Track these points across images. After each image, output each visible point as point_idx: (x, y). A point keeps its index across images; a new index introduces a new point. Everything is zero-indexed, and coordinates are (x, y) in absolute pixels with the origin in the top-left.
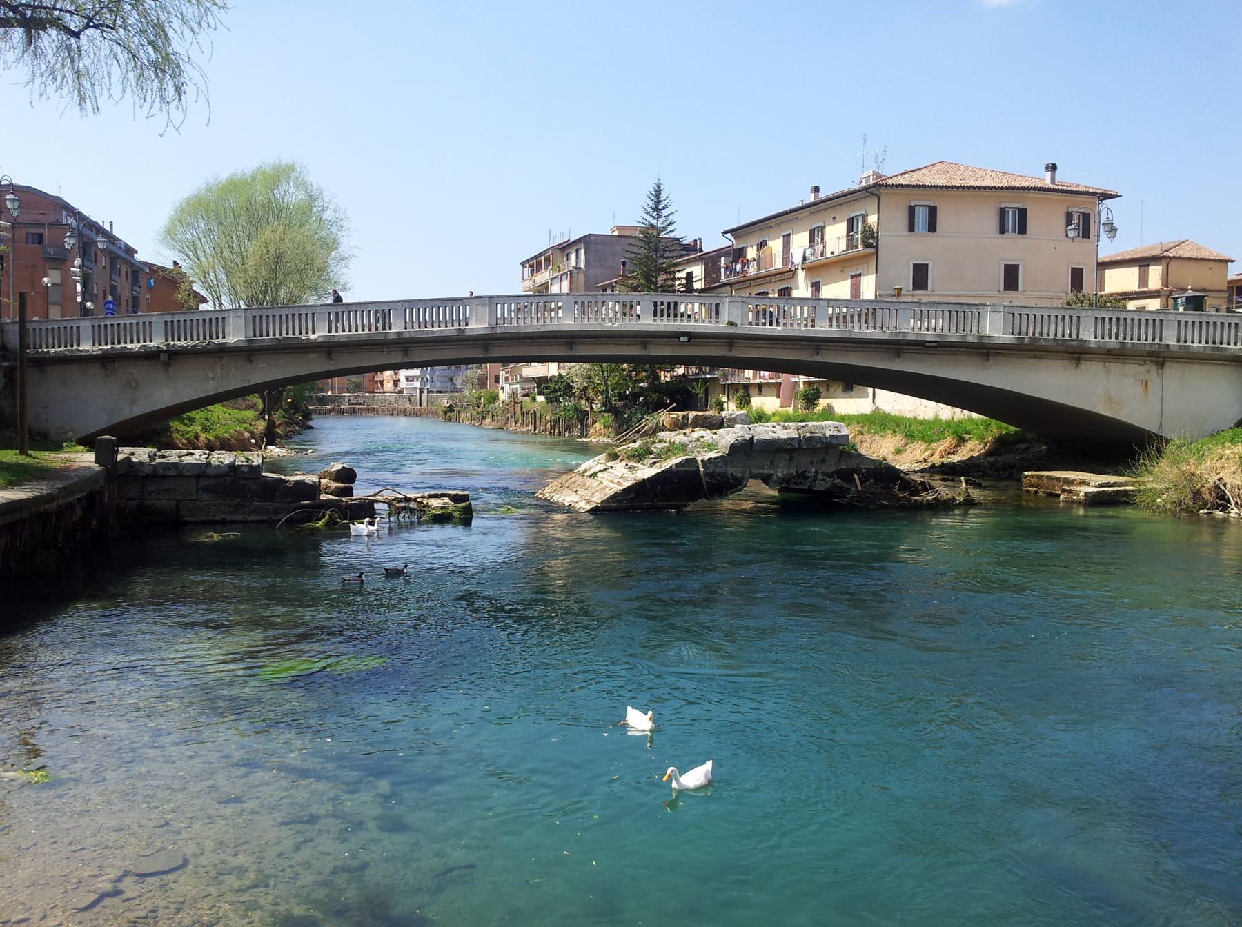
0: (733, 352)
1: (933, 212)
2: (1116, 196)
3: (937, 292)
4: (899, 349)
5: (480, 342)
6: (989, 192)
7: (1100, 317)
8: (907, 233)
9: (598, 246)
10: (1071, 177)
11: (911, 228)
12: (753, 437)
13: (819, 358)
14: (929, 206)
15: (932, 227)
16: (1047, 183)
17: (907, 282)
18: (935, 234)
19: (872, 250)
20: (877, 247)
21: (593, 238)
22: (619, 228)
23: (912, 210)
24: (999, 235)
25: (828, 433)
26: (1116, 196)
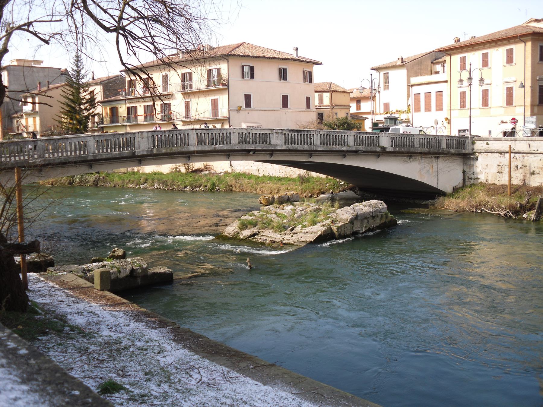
0: (272, 158)
1: (252, 69)
2: (321, 64)
3: (256, 109)
4: (345, 154)
5: (138, 159)
6: (275, 60)
7: (421, 138)
8: (241, 79)
9: (15, 72)
10: (303, 54)
11: (243, 76)
12: (357, 214)
13: (311, 160)
14: (250, 66)
15: (252, 77)
16: (295, 56)
17: (243, 105)
18: (253, 80)
19: (226, 87)
20: (228, 86)
21: (12, 67)
22: (18, 60)
23: (243, 67)
24: (279, 81)
25: (381, 207)
26: (321, 64)
